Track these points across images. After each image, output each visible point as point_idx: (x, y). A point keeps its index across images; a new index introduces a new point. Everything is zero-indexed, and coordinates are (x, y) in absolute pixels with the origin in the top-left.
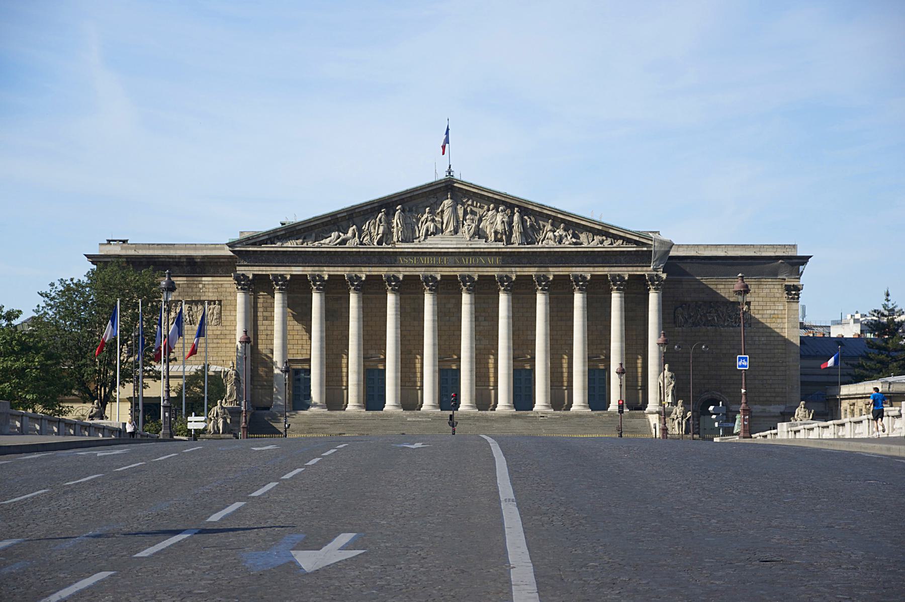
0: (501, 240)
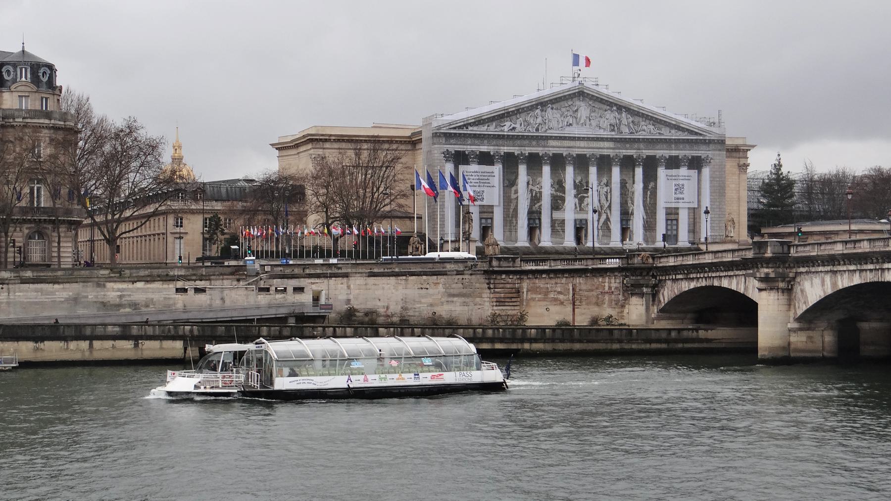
0: (613, 130)
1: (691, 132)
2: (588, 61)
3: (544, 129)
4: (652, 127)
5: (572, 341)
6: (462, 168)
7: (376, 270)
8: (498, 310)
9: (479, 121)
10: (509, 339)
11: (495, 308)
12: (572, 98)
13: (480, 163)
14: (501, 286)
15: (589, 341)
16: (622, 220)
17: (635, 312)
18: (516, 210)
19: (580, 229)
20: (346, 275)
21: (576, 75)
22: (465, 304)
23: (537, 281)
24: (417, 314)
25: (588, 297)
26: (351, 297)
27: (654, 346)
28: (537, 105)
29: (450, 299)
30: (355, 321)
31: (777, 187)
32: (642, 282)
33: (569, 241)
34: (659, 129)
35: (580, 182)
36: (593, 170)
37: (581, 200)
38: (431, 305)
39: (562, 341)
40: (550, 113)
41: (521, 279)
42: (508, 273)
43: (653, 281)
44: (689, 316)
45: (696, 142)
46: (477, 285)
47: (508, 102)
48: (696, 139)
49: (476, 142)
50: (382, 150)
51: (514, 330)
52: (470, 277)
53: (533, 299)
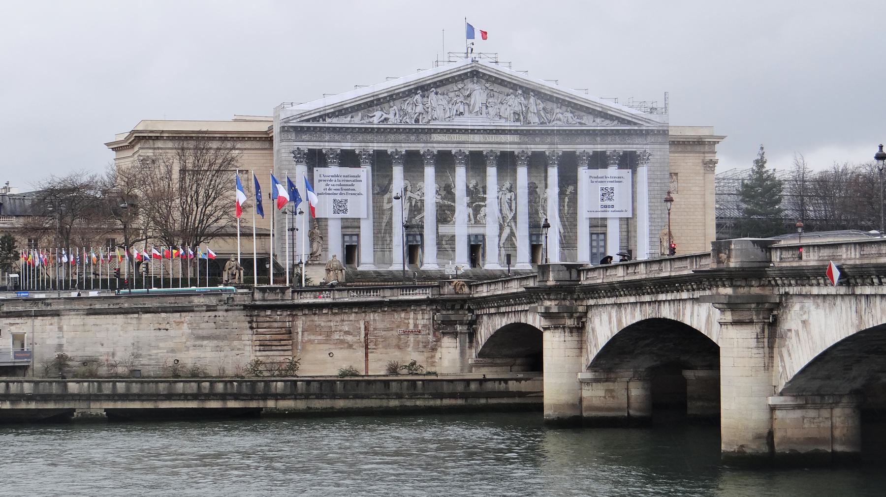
0: (518, 120)
1: (622, 121)
2: (484, 34)
3: (425, 120)
4: (569, 115)
5: (334, 396)
6: (318, 171)
7: (97, 306)
8: (261, 356)
9: (340, 111)
10: (246, 395)
11: (258, 354)
12: (463, 80)
13: (342, 164)
14: (266, 325)
15: (356, 397)
16: (531, 235)
17: (449, 359)
18: (390, 224)
19: (475, 250)
20: (56, 314)
21: (470, 51)
22: (219, 349)
23: (316, 318)
24: (153, 362)
25: (385, 339)
26: (64, 341)
27: (447, 402)
28: (417, 89)
29: (198, 343)
30: (69, 372)
31: (760, 189)
32: (453, 318)
33: (461, 261)
34: (579, 117)
35: (475, 187)
36: (492, 172)
37: (477, 210)
38: (173, 351)
39: (319, 396)
40: (433, 99)
41: (293, 316)
42: (273, 308)
43: (469, 317)
44: (519, 361)
45: (629, 133)
46: (235, 324)
47: (380, 86)
48: (628, 128)
49: (337, 137)
50: (204, 149)
51: (253, 383)
52: (225, 314)
53: (311, 342)
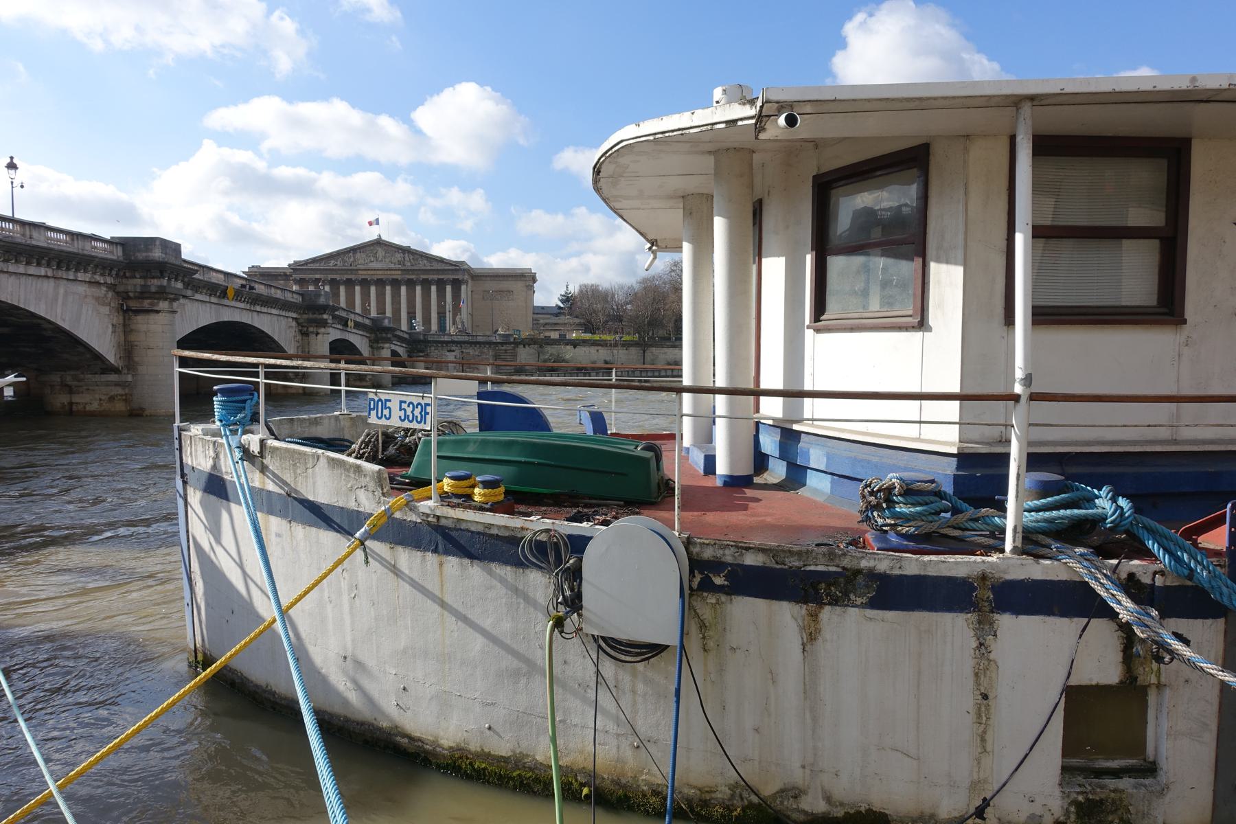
9: (314, 260)
40: (358, 255)
